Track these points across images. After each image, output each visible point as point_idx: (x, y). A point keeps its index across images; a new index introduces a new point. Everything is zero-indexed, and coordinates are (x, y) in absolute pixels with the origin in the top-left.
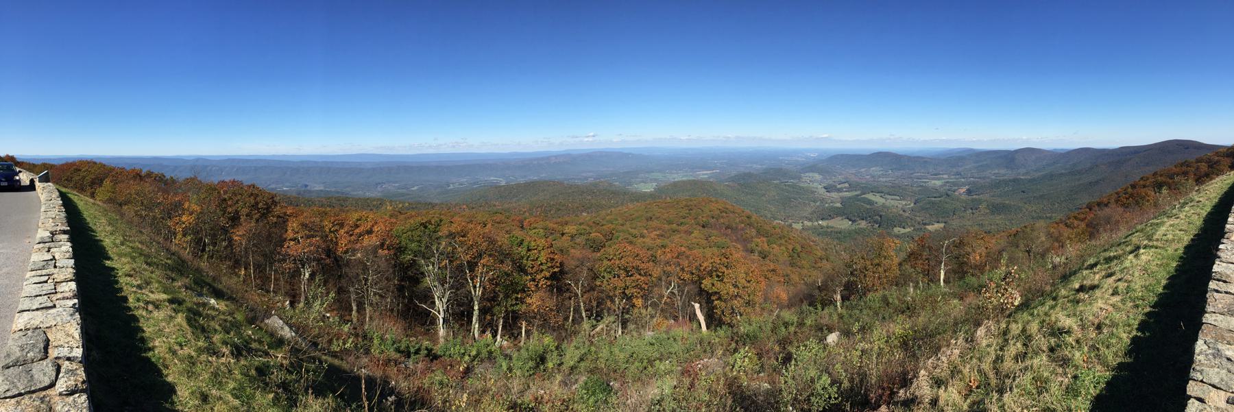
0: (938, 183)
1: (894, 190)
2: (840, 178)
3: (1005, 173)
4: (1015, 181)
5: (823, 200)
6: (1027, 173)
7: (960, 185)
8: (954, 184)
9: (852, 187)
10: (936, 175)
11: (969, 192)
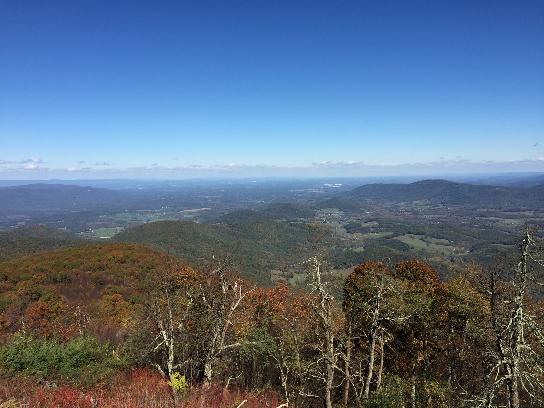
0: (514, 223)
1: (441, 231)
2: (369, 214)
5: (340, 243)
9: (382, 226)
10: (513, 212)
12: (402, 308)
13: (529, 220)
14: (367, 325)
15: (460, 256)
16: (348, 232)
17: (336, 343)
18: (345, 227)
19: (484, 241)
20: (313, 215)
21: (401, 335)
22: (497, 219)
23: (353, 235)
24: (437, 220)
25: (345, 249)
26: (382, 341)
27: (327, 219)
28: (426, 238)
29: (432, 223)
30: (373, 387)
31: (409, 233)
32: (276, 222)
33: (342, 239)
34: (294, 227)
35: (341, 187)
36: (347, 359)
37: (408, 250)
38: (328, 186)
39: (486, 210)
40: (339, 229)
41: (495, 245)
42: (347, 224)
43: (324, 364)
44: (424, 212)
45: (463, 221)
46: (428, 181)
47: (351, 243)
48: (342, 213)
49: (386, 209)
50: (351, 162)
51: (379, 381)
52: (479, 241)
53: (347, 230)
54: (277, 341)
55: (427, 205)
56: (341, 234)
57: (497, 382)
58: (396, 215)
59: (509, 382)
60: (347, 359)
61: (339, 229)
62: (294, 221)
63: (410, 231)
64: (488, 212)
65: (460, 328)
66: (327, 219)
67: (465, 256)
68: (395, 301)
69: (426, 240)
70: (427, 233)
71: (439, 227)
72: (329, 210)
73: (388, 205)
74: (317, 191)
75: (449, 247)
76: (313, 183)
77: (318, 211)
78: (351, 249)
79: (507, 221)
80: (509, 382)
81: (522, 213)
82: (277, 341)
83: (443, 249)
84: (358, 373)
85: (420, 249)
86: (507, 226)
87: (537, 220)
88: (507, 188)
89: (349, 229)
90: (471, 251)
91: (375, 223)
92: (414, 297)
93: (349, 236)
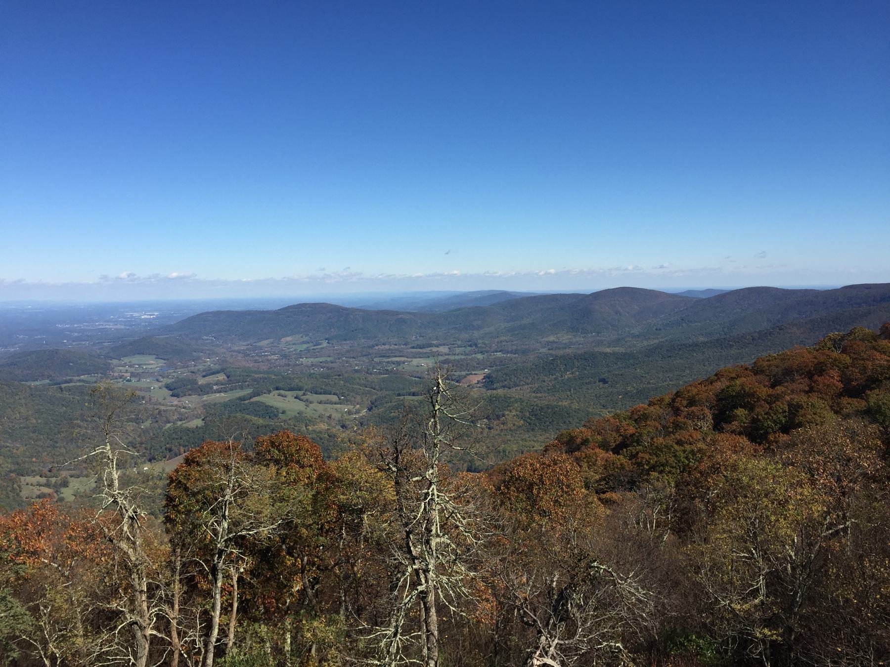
0: (425, 363)
1: (325, 384)
2: (209, 362)
3: (567, 341)
4: (589, 358)
5: (158, 416)
6: (618, 342)
7: (470, 367)
8: (459, 365)
9: (233, 380)
10: (422, 348)
11: (489, 382)
12: (267, 511)
13: (441, 358)
14: (208, 550)
15: (355, 418)
16: (172, 396)
17: (152, 590)
18: (168, 387)
19: (387, 393)
20: (105, 370)
21: (266, 556)
22: (403, 359)
23: (183, 399)
24: (320, 365)
25: (168, 425)
26: (235, 570)
27: (133, 375)
28: (304, 394)
29: (312, 371)
30: (220, 651)
31: (277, 389)
32: (29, 387)
33: (162, 408)
34: (66, 394)
35: (158, 318)
36: (173, 615)
37: (276, 416)
38: (132, 316)
39: (387, 347)
40: (158, 392)
41: (402, 398)
42: (169, 381)
43: (129, 635)
44: (300, 355)
45: (356, 365)
46: (304, 305)
47: (180, 413)
48: (161, 363)
49: (239, 352)
50: (174, 275)
51: (231, 639)
52: (379, 393)
53: (171, 392)
54: (35, 610)
55: (304, 343)
56: (160, 400)
57: (408, 598)
58: (256, 361)
59: (423, 595)
60: (173, 615)
61: (158, 392)
62: (67, 382)
63: (280, 385)
64: (389, 349)
65: (355, 528)
66: (133, 375)
67: (362, 418)
68: (255, 501)
69: (304, 398)
70: (306, 387)
71: (323, 377)
72: (136, 359)
73: (242, 346)
74: (111, 326)
75: (339, 406)
76: (103, 312)
77: (115, 362)
78: (179, 423)
79: (415, 361)
80: (423, 595)
81: (435, 349)
82: (35, 610)
83: (329, 410)
84: (194, 635)
85: (295, 414)
86: (417, 369)
87: (452, 358)
88: (414, 314)
89: (175, 390)
90: (370, 409)
91: (221, 377)
92: (286, 491)
93: (175, 401)
